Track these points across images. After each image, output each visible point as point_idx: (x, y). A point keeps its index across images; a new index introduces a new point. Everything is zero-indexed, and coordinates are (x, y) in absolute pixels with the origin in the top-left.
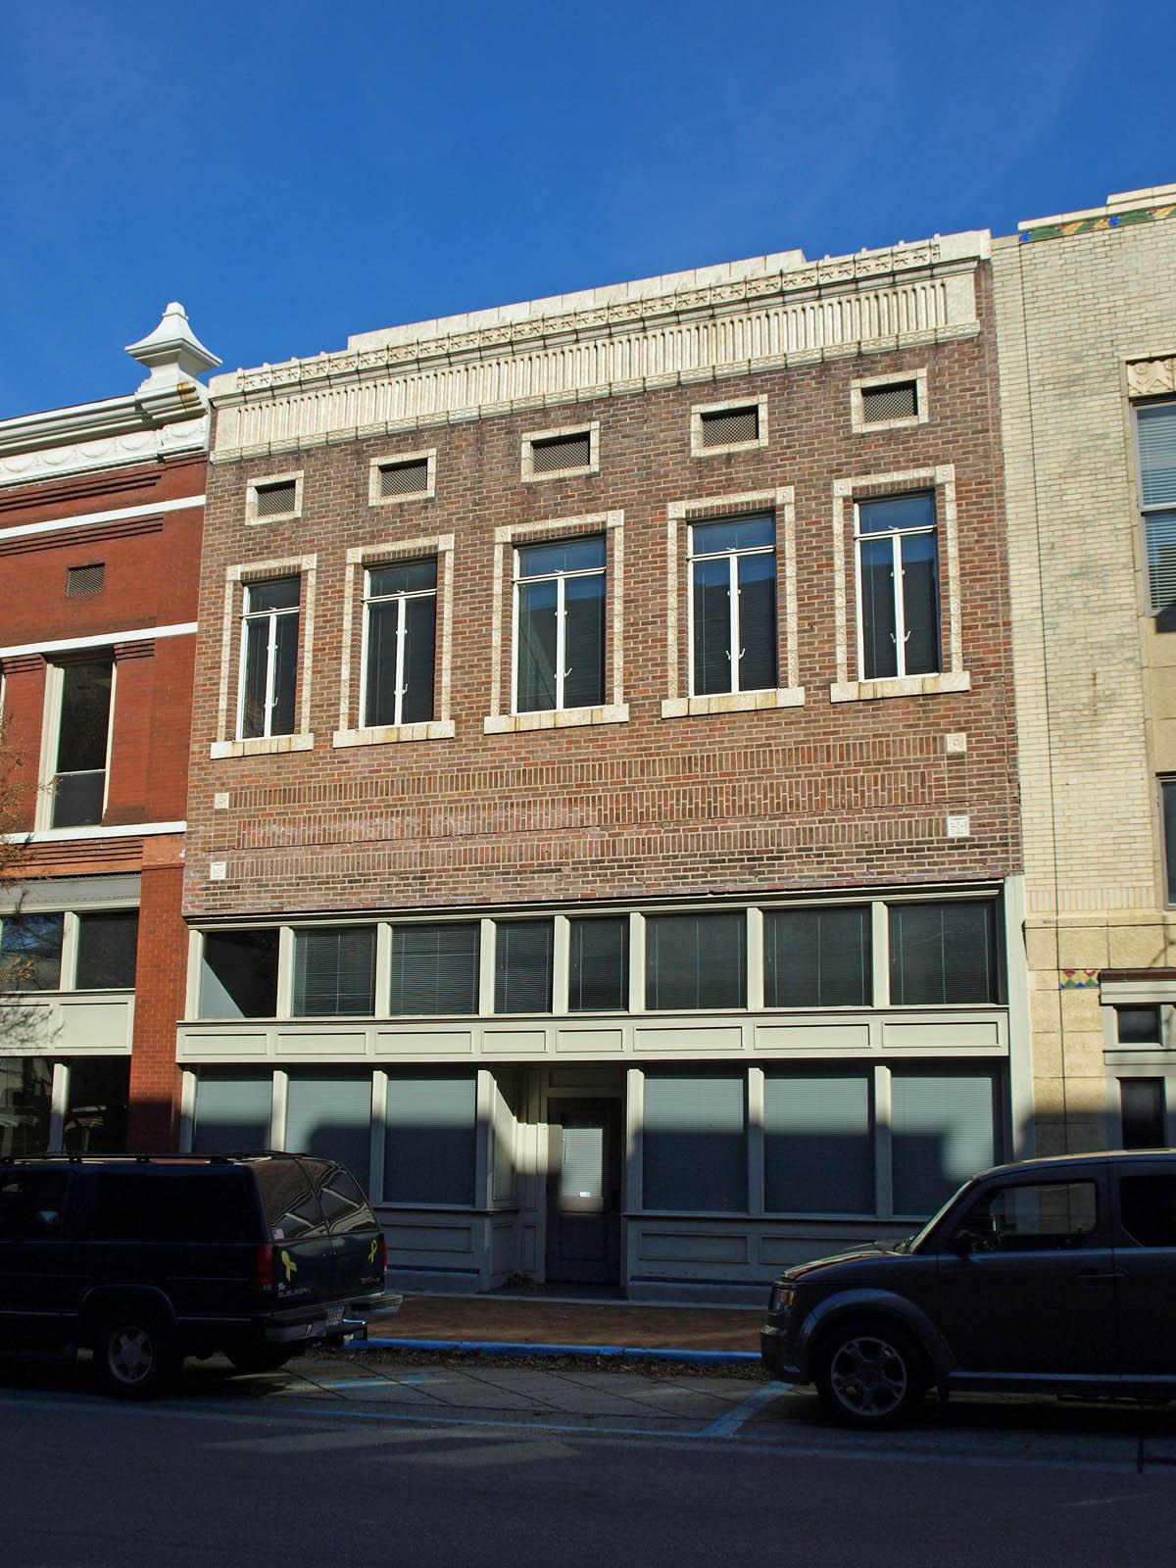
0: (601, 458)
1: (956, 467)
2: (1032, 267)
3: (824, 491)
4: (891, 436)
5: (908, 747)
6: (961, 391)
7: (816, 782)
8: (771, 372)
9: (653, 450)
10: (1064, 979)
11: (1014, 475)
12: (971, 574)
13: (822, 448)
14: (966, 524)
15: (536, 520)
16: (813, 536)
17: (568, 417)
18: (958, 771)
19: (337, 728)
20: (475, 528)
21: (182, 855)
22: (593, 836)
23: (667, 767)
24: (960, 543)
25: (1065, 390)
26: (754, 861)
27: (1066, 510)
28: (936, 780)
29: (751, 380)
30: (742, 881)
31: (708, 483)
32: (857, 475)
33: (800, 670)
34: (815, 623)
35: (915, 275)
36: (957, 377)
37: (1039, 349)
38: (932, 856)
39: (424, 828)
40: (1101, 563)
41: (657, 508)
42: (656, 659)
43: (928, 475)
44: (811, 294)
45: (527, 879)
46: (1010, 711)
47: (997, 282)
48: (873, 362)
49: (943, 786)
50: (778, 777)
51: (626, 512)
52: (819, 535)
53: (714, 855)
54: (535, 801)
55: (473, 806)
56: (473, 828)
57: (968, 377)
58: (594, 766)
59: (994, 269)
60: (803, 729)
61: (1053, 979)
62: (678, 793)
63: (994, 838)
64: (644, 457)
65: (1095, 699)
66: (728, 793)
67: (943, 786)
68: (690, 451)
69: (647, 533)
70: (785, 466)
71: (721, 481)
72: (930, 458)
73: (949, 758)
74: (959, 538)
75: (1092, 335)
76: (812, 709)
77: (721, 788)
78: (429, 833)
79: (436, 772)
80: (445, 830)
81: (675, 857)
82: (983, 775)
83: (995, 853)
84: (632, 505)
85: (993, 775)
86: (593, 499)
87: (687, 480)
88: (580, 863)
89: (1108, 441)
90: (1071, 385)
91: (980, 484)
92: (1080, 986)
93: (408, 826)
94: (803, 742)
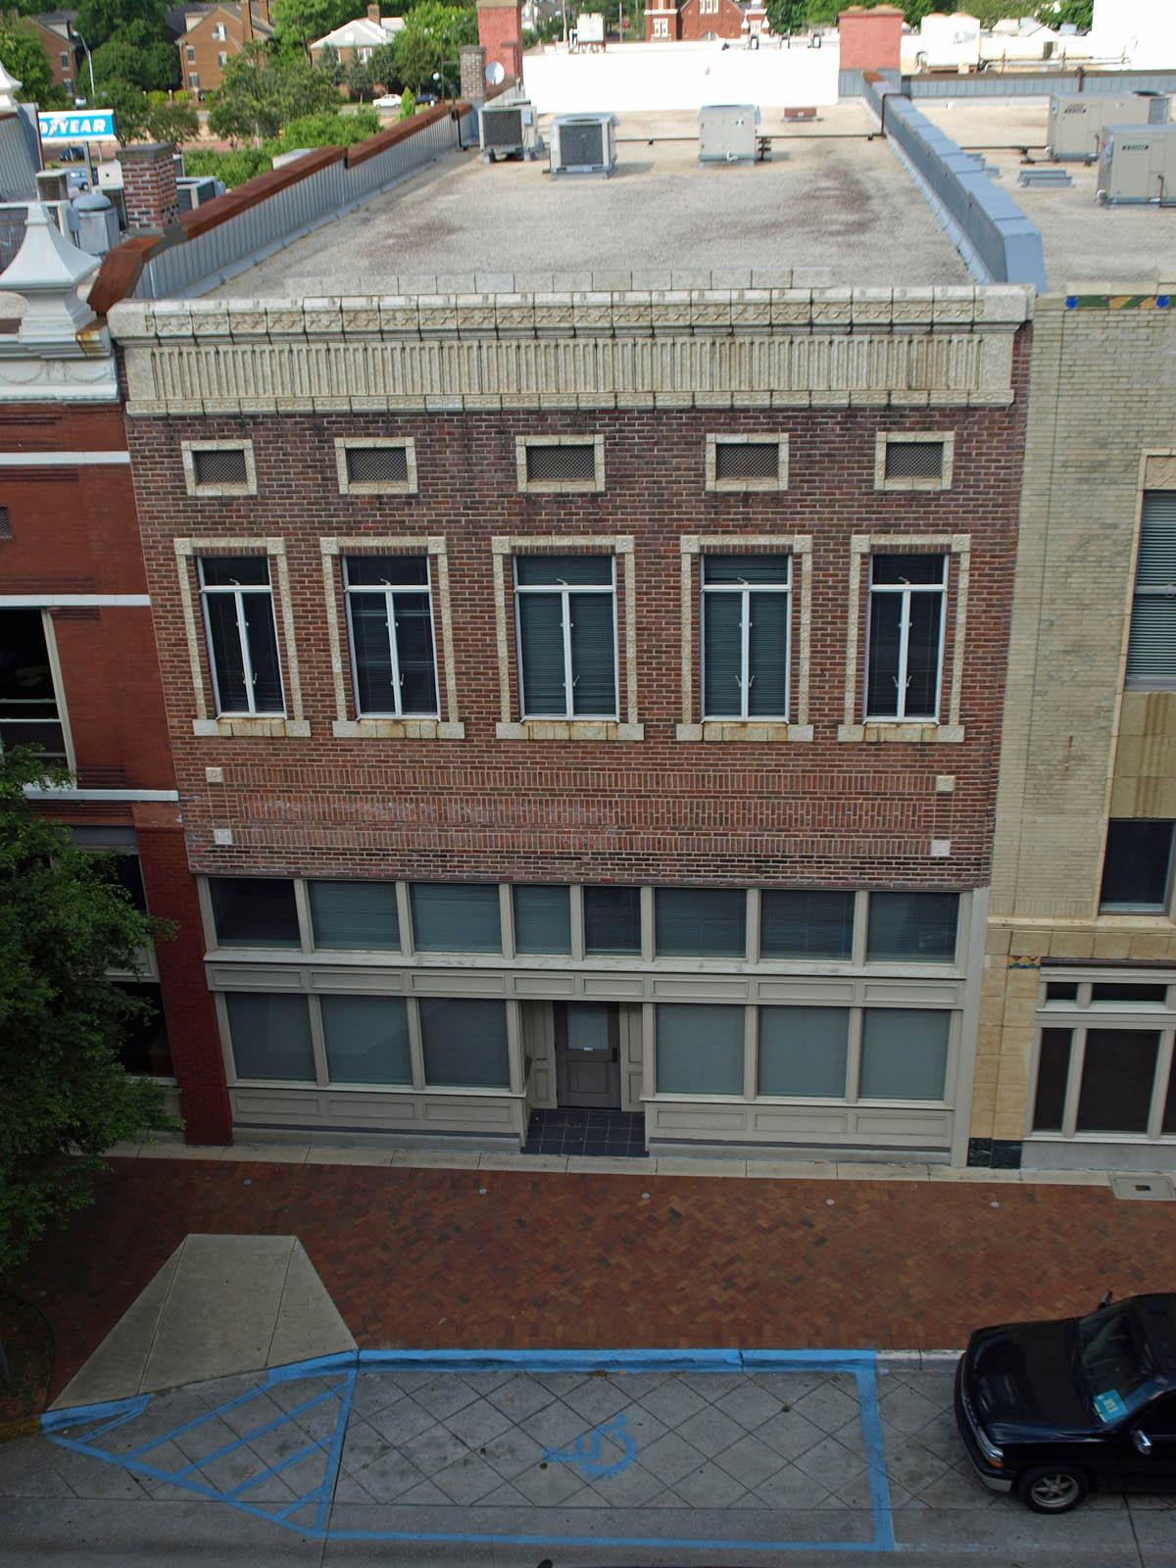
0: (607, 476)
1: (973, 537)
2: (1074, 338)
3: (842, 544)
4: (912, 497)
5: (904, 783)
6: (986, 461)
7: (820, 804)
8: (794, 409)
9: (665, 476)
10: (1013, 962)
11: (1027, 550)
12: (975, 640)
13: (843, 500)
14: (976, 594)
15: (538, 534)
16: (830, 587)
17: (568, 425)
18: (945, 805)
19: (336, 719)
20: (469, 533)
21: (180, 820)
22: (611, 832)
23: (681, 781)
24: (969, 611)
25: (1085, 476)
26: (761, 864)
27: (1068, 591)
28: (925, 811)
29: (772, 417)
30: (751, 877)
31: (724, 520)
32: (876, 532)
33: (811, 710)
34: (826, 670)
35: (954, 328)
36: (985, 446)
37: (1068, 429)
38: (916, 869)
39: (440, 815)
40: (1093, 643)
41: (670, 539)
42: (670, 686)
43: (946, 542)
44: (842, 329)
45: (549, 863)
46: (995, 760)
47: (1036, 348)
48: (902, 416)
49: (931, 816)
50: (785, 798)
51: (636, 538)
52: (836, 588)
53: (724, 855)
54: (553, 801)
55: (490, 800)
56: (490, 817)
57: (996, 448)
58: (610, 776)
59: (1035, 332)
60: (811, 760)
61: (1004, 961)
62: (692, 803)
63: (970, 859)
64: (655, 482)
65: (1067, 759)
66: (738, 808)
67: (931, 816)
68: (705, 482)
69: (660, 564)
70: (804, 513)
71: (738, 520)
72: (949, 525)
73: (939, 794)
74: (968, 605)
75: (1120, 422)
76: (819, 744)
77: (732, 803)
78: (446, 818)
79: (449, 768)
80: (463, 818)
81: (690, 855)
82: (966, 811)
83: (969, 870)
84: (644, 533)
85: (975, 811)
86: (600, 520)
87: (702, 513)
88: (599, 854)
89: (1117, 532)
90: (1092, 471)
91: (994, 557)
92: (1024, 967)
93: (423, 812)
94: (810, 771)
